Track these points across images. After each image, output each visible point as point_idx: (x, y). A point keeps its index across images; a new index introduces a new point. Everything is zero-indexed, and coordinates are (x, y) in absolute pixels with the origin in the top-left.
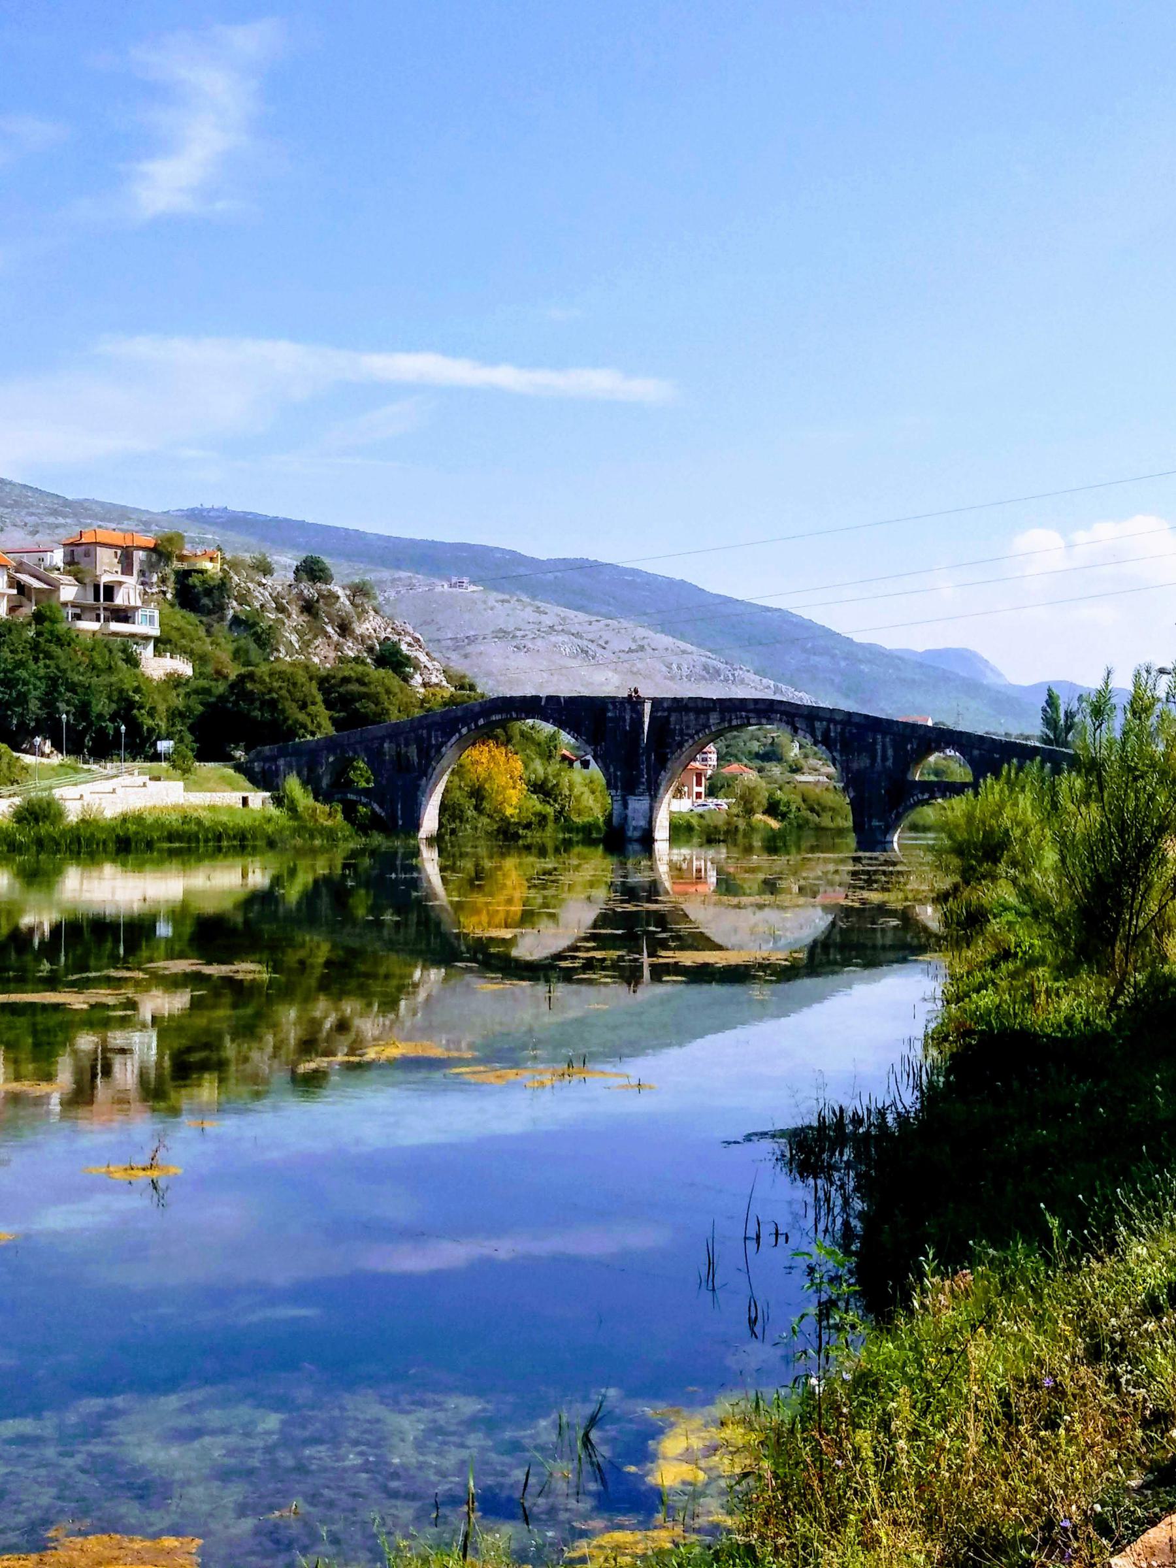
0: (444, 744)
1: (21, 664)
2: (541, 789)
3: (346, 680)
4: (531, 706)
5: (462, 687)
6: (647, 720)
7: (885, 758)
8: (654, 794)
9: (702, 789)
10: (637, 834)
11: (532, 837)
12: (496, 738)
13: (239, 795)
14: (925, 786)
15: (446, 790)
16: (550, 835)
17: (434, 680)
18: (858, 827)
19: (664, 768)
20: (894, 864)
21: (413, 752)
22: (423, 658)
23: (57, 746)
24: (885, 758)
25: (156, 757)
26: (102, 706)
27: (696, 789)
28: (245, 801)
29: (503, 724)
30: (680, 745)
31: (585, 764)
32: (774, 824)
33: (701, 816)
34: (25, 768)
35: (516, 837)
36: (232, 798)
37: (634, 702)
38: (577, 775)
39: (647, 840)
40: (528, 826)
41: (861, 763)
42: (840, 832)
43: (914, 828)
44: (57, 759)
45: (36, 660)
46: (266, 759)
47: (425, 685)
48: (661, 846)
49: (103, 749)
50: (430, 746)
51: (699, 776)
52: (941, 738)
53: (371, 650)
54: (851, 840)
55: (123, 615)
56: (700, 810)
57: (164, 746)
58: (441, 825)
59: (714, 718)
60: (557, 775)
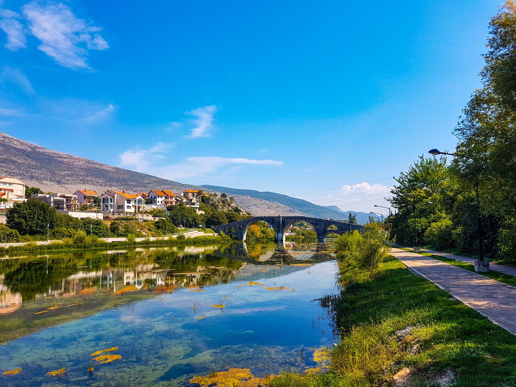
0: (246, 225)
1: (177, 213)
2: (263, 232)
3: (230, 214)
4: (261, 218)
5: (249, 215)
6: (281, 220)
7: (322, 226)
8: (283, 234)
9: (290, 231)
10: (280, 240)
11: (262, 240)
12: (255, 223)
13: (213, 234)
14: (330, 231)
15: (247, 233)
16: (265, 240)
17: (244, 213)
18: (318, 238)
19: (284, 228)
20: (325, 245)
21: (242, 226)
22: (242, 210)
23: (183, 226)
24: (322, 226)
25: (199, 228)
26: (190, 219)
27: (289, 231)
28: (214, 235)
29: (256, 221)
30: (287, 224)
31: (270, 227)
32: (303, 237)
33: (290, 236)
34: (178, 230)
35: (259, 240)
36: (212, 234)
37: (279, 217)
38: (269, 229)
39: (282, 241)
40: (261, 238)
41: (318, 227)
42: (315, 238)
43: (327, 237)
44: (183, 228)
45: (180, 212)
46: (217, 228)
47: (242, 214)
48: (284, 242)
49: (191, 226)
50: (244, 225)
51: (290, 229)
52: (331, 222)
53: (233, 209)
54: (317, 240)
55: (194, 204)
56: (290, 235)
57: (200, 226)
58: (246, 239)
59: (293, 220)
60: (266, 230)
